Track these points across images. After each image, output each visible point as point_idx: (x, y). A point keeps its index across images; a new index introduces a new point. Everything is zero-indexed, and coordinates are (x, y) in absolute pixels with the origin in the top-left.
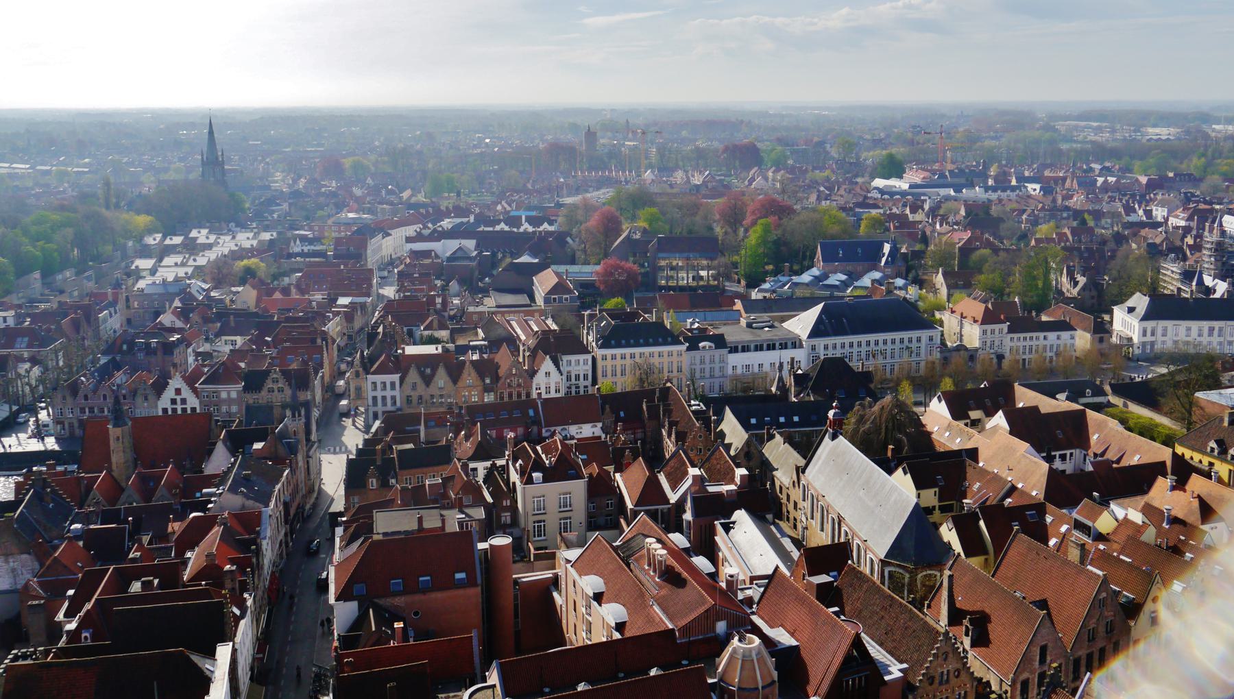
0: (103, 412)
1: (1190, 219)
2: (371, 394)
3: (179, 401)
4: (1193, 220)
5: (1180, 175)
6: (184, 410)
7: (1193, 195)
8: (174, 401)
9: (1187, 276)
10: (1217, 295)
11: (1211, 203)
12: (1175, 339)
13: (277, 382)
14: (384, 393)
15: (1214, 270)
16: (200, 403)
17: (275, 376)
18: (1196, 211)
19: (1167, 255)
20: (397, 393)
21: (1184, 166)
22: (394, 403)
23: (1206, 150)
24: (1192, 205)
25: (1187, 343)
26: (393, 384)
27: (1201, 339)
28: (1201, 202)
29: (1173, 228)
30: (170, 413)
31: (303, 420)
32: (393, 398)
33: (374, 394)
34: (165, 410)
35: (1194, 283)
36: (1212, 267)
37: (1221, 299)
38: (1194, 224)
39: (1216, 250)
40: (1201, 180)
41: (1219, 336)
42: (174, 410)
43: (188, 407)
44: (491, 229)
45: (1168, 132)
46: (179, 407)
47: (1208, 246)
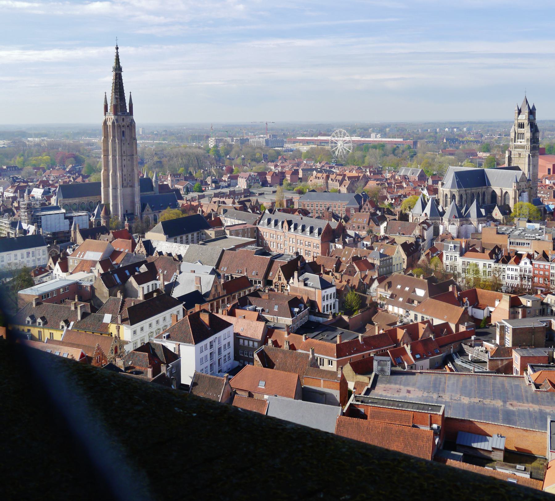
1: (15, 192)
4: (17, 192)
5: (10, 167)
7: (17, 178)
9: (13, 225)
10: (30, 234)
11: (27, 182)
12: (9, 262)
15: (28, 219)
18: (18, 187)
19: (4, 214)
21: (12, 162)
23: (24, 153)
24: (17, 184)
25: (16, 264)
27: (22, 260)
28: (20, 182)
29: (7, 198)
35: (17, 229)
36: (26, 218)
37: (32, 236)
38: (18, 195)
39: (28, 208)
40: (21, 169)
41: (33, 256)
45: (3, 143)
47: (23, 206)
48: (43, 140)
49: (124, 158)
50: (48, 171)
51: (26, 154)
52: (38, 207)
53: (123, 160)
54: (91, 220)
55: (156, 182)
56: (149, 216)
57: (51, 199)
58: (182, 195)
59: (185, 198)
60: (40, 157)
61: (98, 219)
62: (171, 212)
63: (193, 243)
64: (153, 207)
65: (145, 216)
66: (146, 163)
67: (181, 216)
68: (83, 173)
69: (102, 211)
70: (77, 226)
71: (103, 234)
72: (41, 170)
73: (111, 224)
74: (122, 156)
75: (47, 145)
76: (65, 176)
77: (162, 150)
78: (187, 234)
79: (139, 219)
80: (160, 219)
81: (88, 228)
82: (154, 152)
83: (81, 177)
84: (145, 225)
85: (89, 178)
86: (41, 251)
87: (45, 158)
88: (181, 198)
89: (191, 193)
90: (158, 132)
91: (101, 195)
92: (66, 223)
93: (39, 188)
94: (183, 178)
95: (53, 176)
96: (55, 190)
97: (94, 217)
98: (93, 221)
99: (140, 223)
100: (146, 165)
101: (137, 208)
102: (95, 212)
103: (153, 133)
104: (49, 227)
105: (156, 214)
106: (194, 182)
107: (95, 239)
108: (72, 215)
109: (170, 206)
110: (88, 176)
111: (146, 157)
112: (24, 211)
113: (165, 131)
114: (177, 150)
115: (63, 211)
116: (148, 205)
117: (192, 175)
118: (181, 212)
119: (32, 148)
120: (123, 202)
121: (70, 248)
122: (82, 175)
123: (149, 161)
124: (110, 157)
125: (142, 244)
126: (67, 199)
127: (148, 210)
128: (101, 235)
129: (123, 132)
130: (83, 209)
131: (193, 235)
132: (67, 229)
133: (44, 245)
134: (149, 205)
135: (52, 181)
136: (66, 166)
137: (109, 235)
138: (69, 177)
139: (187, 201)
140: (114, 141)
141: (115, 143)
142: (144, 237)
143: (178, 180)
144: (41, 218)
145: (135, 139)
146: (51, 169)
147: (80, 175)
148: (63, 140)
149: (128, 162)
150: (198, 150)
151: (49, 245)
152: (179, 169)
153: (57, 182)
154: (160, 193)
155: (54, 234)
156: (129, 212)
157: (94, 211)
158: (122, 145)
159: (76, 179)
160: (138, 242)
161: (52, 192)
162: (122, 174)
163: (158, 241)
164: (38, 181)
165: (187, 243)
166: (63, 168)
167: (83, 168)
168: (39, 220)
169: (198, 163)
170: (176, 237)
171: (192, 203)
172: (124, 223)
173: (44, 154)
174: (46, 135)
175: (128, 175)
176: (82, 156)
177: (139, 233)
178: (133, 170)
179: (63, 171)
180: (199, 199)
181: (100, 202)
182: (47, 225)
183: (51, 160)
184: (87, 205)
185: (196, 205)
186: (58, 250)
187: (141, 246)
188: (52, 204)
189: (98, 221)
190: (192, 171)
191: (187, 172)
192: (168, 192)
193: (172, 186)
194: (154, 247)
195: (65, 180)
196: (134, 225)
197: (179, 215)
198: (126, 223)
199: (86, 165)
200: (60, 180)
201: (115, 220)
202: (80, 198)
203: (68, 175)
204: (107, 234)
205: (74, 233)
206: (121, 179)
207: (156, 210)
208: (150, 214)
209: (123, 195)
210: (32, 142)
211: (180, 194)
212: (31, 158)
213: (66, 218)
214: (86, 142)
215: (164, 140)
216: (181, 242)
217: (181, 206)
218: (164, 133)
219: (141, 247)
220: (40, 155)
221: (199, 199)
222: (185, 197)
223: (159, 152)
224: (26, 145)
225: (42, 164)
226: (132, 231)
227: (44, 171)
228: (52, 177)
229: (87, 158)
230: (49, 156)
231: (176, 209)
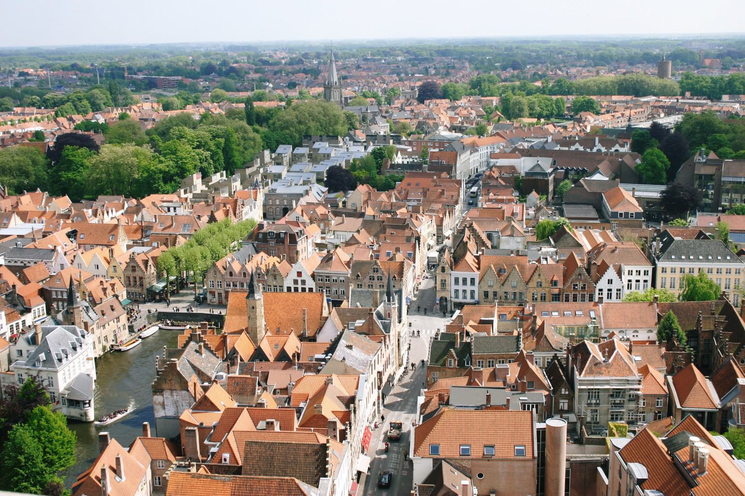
0: (243, 286)
2: (454, 287)
3: (300, 282)
6: (304, 290)
8: (296, 282)
13: (377, 271)
14: (465, 288)
16: (316, 284)
17: (375, 267)
20: (475, 288)
22: (472, 297)
26: (473, 281)
30: (293, 290)
31: (397, 305)
32: (472, 292)
33: (457, 287)
34: (289, 289)
42: (296, 290)
43: (307, 287)
44: (567, 149)
46: (300, 286)
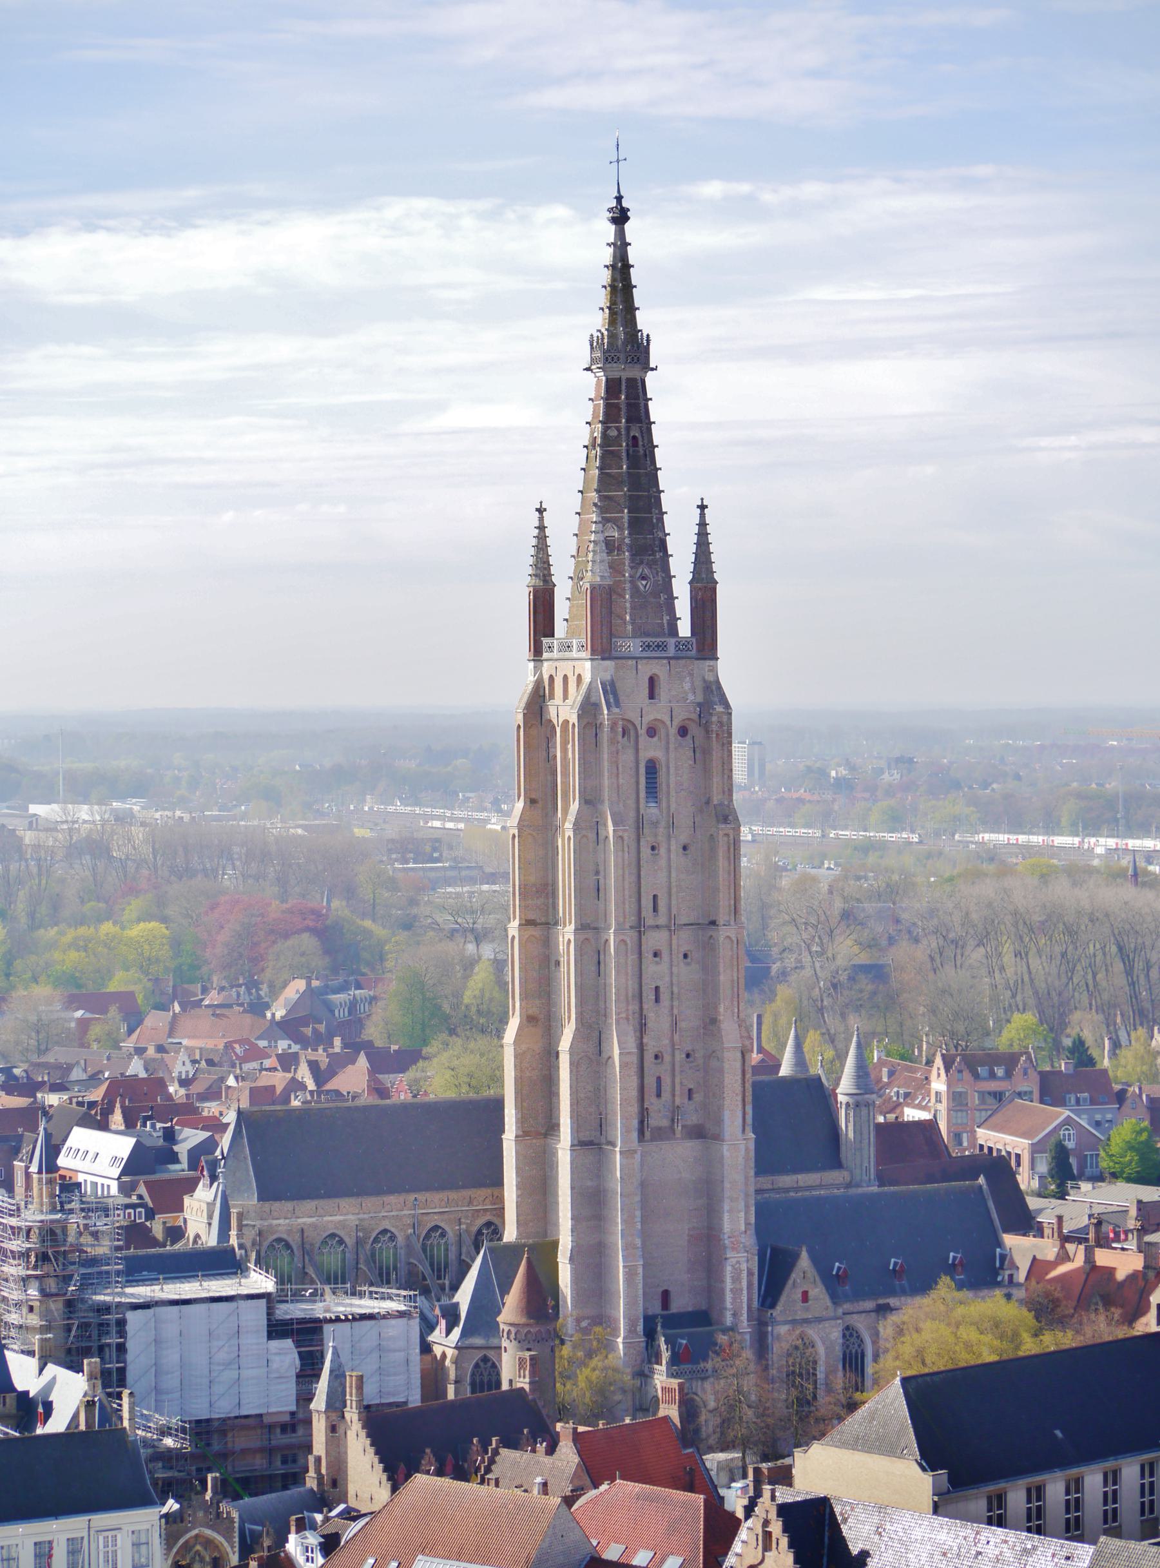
10: (57, 1424)
36: (34, 1320)
37: (69, 1437)
39: (43, 1258)
47: (16, 1245)
48: (122, 819)
49: (655, 940)
50: (156, 1021)
51: (20, 907)
52: (103, 1249)
53: (648, 956)
54: (438, 1350)
55: (859, 1105)
56: (812, 1332)
57: (187, 1200)
58: (1033, 1203)
59: (1046, 1219)
60: (107, 927)
61: (478, 1341)
62: (960, 1310)
63: (1116, 1533)
64: (840, 1278)
65: (782, 1334)
66: (784, 974)
67: (1029, 1346)
68: (374, 1032)
69: (505, 1289)
70: (350, 1383)
71: (512, 1443)
72: (113, 1012)
73: (568, 1377)
74: (640, 927)
75: (146, 850)
76: (262, 1054)
77: (892, 892)
78: (1074, 1472)
79: (748, 1354)
80: (887, 1361)
81: (415, 1399)
82: (838, 905)
83: (362, 1062)
84: (781, 1395)
85: (412, 1073)
86: (124, 1542)
87: (137, 931)
88: (1026, 1223)
89: (1085, 1186)
90: (852, 768)
91: (499, 1182)
92: (276, 1362)
93: (103, 1126)
94: (1031, 1085)
95: (190, 1050)
96: (208, 1146)
97: (457, 1332)
98: (450, 1353)
99: (749, 1384)
100: (784, 992)
101: (736, 1279)
102: (464, 1297)
103: (823, 773)
104: (171, 1381)
105: (861, 1324)
106: (1108, 1112)
107: (462, 1475)
108: (318, 1310)
109: (951, 1270)
110: (406, 1059)
111: (780, 934)
112: (21, 1271)
113: (904, 762)
114: (987, 889)
115: (261, 1281)
116: (804, 1261)
117: (1091, 1062)
118: (1029, 1317)
119: (59, 871)
120: (645, 1235)
121: (301, 1527)
122: (368, 1047)
123: (799, 967)
124: (567, 934)
125: (776, 1527)
126: (288, 1205)
127: (805, 1297)
128: (504, 1452)
129: (652, 769)
130: (383, 1277)
131: (1112, 1477)
132: (282, 1401)
133: (141, 1500)
134: (815, 1260)
135: (184, 1083)
136: (264, 990)
137: (551, 1450)
138: (288, 1061)
139: (1065, 1239)
140: (589, 827)
141: (599, 839)
142: (784, 1477)
143: (998, 1096)
144: (122, 1323)
145: (727, 816)
146: (177, 1008)
147: (354, 1047)
148: (244, 817)
149: (687, 973)
150: (1128, 892)
151: (172, 1505)
152: (1002, 1023)
153: (213, 1093)
154: (882, 1180)
155: (201, 1430)
156: (680, 1304)
157: (455, 1288)
158: (646, 851)
159: (332, 1072)
160: (749, 1510)
161: (184, 1157)
162: (641, 1047)
163: (881, 1508)
164: (94, 1079)
165: (1074, 1530)
166: (245, 999)
167: (373, 999)
168: (113, 1340)
169: (1132, 984)
170: (1002, 1485)
171: (1103, 1257)
172: (644, 1375)
173: (134, 906)
174: (139, 788)
175: (680, 1056)
176: (368, 923)
177: (744, 1445)
178: (711, 1023)
179: (248, 1019)
180: (1143, 1231)
181: (494, 1229)
182: (158, 1370)
183: (176, 944)
184: (409, 1246)
185: (1133, 1277)
186: (229, 1539)
187: (768, 1535)
188: (191, 1233)
189: (478, 1356)
190: (1088, 1036)
191: (1057, 1046)
192: (931, 1179)
193: (957, 1137)
194: (855, 1551)
195: (265, 1080)
196: (709, 1395)
197: (1015, 1338)
198: (661, 1378)
199: (391, 987)
200: (231, 1081)
201: (590, 1355)
202: (370, 1202)
203: (283, 1045)
204: (541, 1447)
205: (333, 1429)
206: (634, 1082)
207: (858, 1296)
208: (820, 1320)
209: (643, 1185)
210: (51, 828)
211: (1018, 1196)
212: (53, 932)
213: (277, 1329)
214: (391, 831)
215: (895, 821)
216: (1036, 1523)
217: (1021, 1277)
218: (891, 777)
219: (767, 1547)
220: (108, 915)
221: (1143, 1231)
222: (1046, 1210)
223: (870, 907)
224: (18, 846)
225: (120, 975)
226: (697, 1431)
227: (134, 1020)
228: (183, 1056)
229: (403, 936)
230: (164, 920)
231: (998, 1293)
